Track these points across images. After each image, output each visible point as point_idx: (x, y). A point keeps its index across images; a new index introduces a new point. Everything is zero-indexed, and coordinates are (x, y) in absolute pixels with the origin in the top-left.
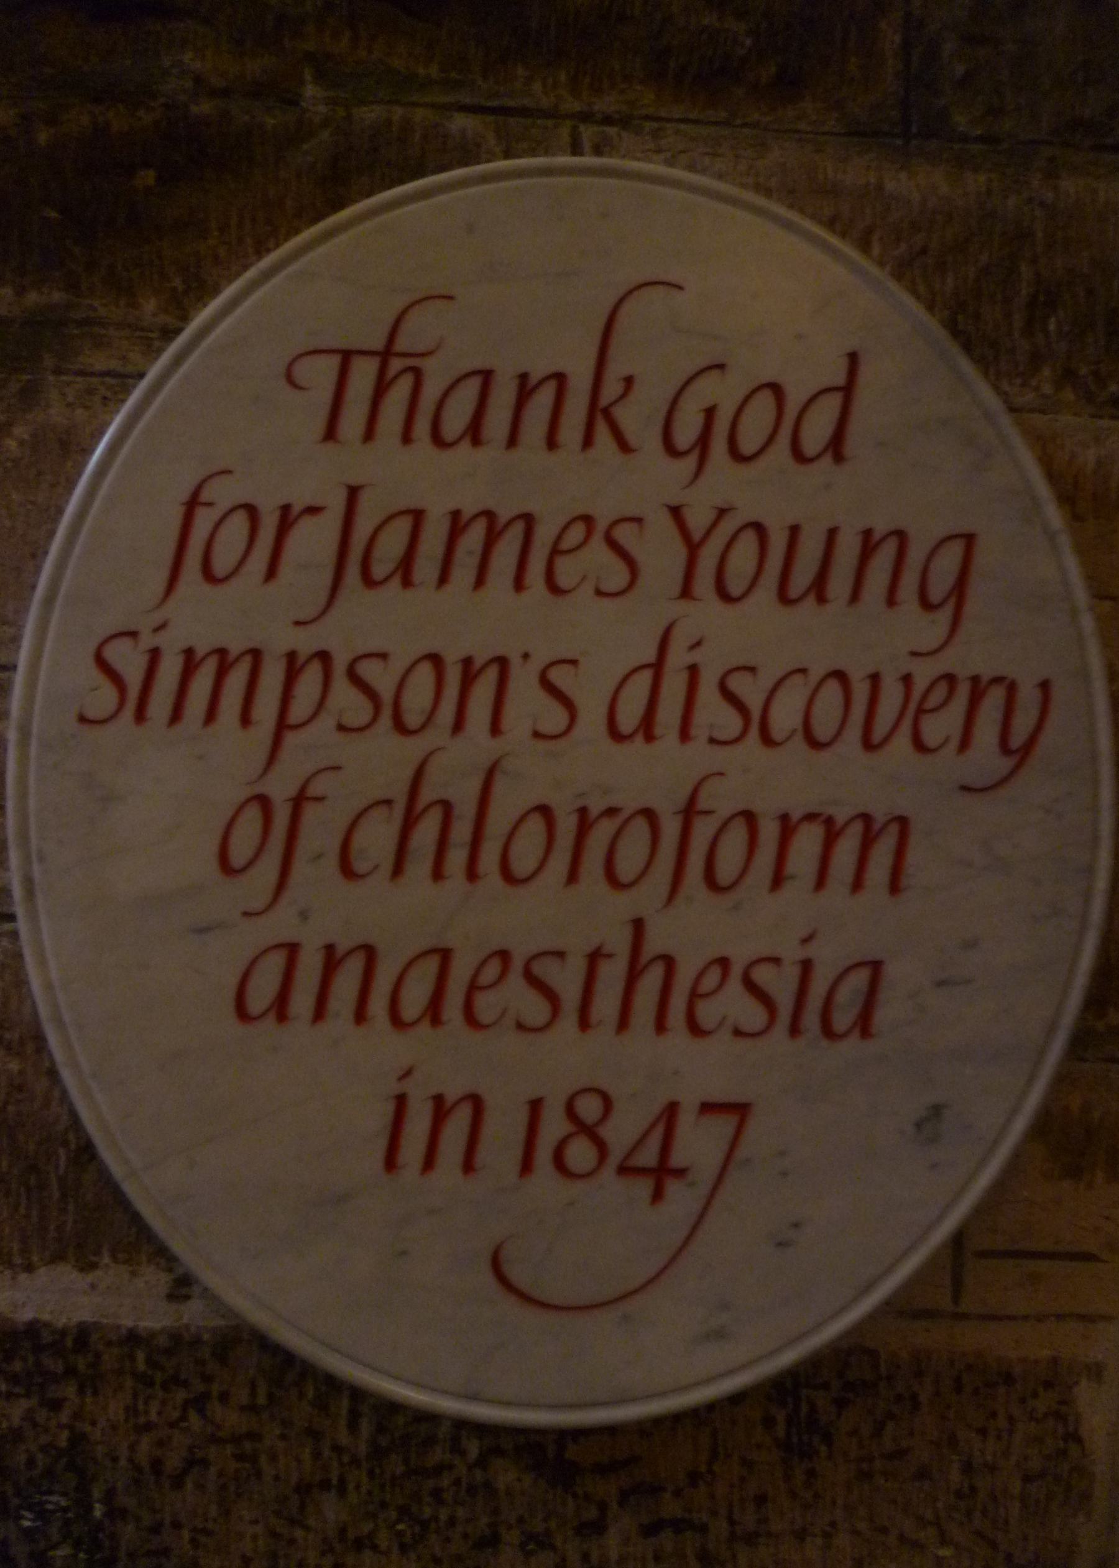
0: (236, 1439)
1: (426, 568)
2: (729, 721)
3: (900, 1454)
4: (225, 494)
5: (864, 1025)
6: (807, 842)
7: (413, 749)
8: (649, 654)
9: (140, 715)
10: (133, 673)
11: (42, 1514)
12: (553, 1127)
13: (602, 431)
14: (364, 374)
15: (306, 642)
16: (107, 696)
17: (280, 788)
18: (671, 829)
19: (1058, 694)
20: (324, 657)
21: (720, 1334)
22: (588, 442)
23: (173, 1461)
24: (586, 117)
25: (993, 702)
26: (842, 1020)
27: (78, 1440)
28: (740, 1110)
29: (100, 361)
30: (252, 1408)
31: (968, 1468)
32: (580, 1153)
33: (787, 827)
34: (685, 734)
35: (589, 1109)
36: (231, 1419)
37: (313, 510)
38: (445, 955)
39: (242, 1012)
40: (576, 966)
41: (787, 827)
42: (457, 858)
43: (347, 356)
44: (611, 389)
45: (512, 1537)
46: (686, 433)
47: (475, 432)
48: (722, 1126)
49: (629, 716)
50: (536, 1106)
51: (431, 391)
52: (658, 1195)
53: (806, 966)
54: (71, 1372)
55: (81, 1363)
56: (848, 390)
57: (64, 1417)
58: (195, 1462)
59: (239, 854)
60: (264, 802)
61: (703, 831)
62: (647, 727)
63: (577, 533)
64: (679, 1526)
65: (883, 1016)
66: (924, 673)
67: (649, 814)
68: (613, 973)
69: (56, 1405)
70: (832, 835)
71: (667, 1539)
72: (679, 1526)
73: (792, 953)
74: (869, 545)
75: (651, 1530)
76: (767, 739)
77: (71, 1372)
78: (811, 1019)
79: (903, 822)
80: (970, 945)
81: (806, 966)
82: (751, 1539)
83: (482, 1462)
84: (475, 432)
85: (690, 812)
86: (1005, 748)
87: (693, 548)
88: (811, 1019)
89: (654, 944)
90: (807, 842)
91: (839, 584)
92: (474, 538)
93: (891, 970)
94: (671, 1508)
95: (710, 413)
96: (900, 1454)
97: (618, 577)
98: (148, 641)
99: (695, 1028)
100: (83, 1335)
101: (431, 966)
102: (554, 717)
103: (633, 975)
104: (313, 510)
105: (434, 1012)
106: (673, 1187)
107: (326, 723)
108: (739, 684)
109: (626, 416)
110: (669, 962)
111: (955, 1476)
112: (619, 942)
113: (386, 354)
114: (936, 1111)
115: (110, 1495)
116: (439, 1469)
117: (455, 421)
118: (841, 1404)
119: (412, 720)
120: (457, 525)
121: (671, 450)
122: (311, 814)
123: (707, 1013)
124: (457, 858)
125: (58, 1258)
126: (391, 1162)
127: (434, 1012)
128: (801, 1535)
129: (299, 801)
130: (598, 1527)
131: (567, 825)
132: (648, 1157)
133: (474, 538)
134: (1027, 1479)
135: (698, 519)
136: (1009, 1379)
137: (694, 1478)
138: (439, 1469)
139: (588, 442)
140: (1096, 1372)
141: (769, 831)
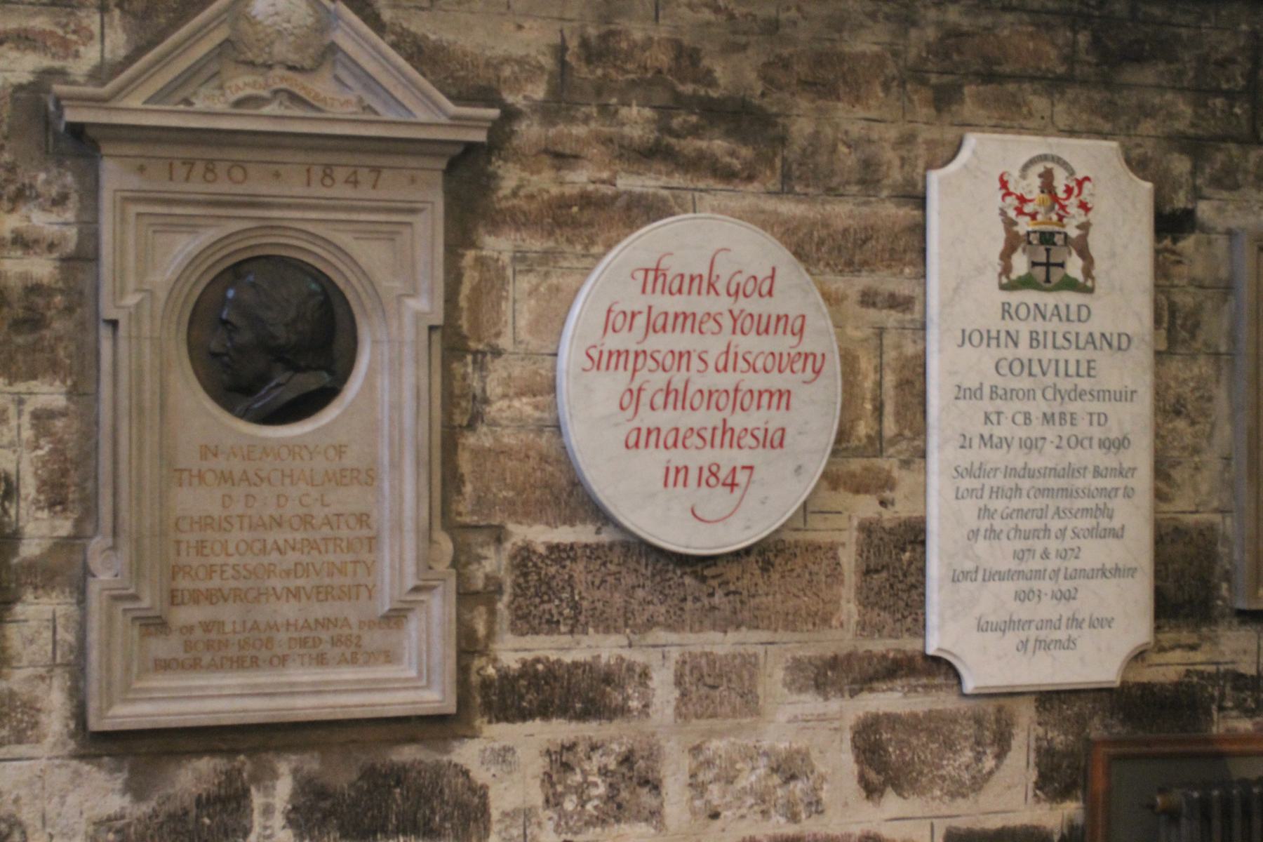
0: (614, 574)
1: (669, 327)
2: (745, 366)
3: (792, 570)
4: (617, 308)
5: (781, 444)
6: (766, 397)
7: (666, 376)
8: (725, 349)
9: (598, 368)
10: (596, 357)
11: (561, 600)
12: (706, 474)
13: (712, 291)
14: (651, 275)
15: (640, 348)
16: (588, 364)
17: (635, 387)
18: (732, 395)
19: (828, 357)
20: (644, 352)
21: (748, 528)
22: (708, 292)
23: (597, 582)
24: (695, 190)
25: (811, 359)
26: (776, 443)
27: (571, 577)
28: (751, 468)
29: (565, 264)
30: (619, 564)
31: (811, 574)
32: (713, 481)
33: (760, 394)
34: (735, 369)
35: (714, 469)
36: (612, 568)
37: (640, 313)
38: (677, 430)
39: (627, 446)
40: (710, 431)
41: (760, 394)
42: (679, 404)
43: (647, 271)
44: (714, 278)
45: (690, 598)
46: (733, 290)
47: (680, 291)
48: (747, 472)
49: (721, 366)
50: (701, 469)
51: (669, 279)
52: (732, 491)
53: (766, 430)
54: (569, 557)
55: (572, 554)
56: (772, 277)
57: (567, 570)
58: (603, 581)
59: (625, 404)
60: (631, 391)
61: (740, 395)
62: (725, 368)
63: (706, 318)
64: (735, 593)
65: (786, 443)
66: (793, 352)
67: (726, 392)
68: (719, 433)
69: (564, 567)
70: (771, 395)
71: (731, 597)
72: (735, 593)
73: (763, 426)
74: (779, 318)
75: (727, 594)
76: (755, 370)
77: (569, 557)
78: (768, 444)
79: (789, 392)
80: (806, 423)
81: (766, 430)
82: (754, 596)
83: (681, 577)
84: (680, 291)
85: (736, 390)
86: (814, 371)
87: (735, 320)
88: (768, 444)
89: (729, 425)
90: (766, 397)
91: (772, 329)
92: (681, 319)
93: (788, 431)
94: (732, 588)
95: (738, 285)
96: (792, 570)
97: (716, 328)
98: (599, 348)
99: (739, 446)
100: (572, 547)
101: (674, 433)
102: (702, 366)
103: (724, 433)
104: (640, 313)
105: (675, 445)
106: (736, 489)
107: (646, 369)
108: (748, 357)
109: (718, 286)
110: (732, 430)
111: (807, 576)
112: (720, 425)
113: (657, 270)
114: (800, 467)
115: (580, 593)
116: (671, 579)
117: (675, 288)
118: (776, 556)
119: (667, 367)
120: (676, 316)
121: (729, 294)
122: (643, 393)
123: (743, 443)
124: (679, 404)
125: (564, 523)
126: (666, 484)
127: (675, 445)
128: (767, 594)
129: (640, 390)
130: (711, 595)
131: (706, 395)
132: (729, 481)
133: (681, 319)
134: (827, 576)
135: (736, 313)
136: (820, 547)
137: (738, 579)
138: (671, 579)
139: (708, 292)
140: (843, 544)
141: (756, 395)
